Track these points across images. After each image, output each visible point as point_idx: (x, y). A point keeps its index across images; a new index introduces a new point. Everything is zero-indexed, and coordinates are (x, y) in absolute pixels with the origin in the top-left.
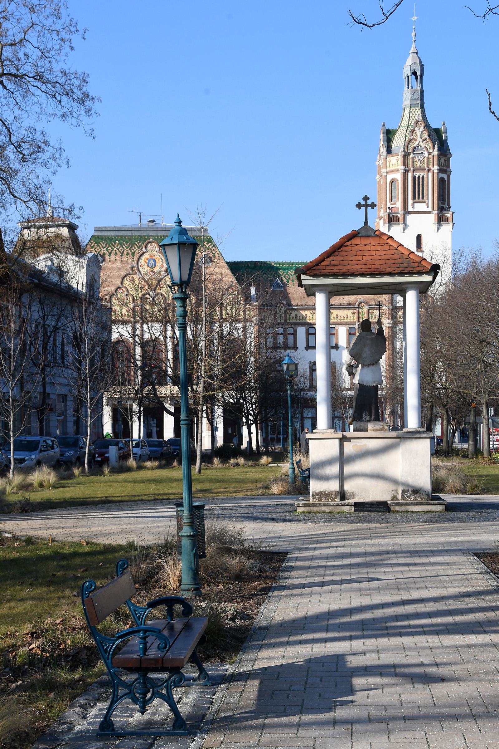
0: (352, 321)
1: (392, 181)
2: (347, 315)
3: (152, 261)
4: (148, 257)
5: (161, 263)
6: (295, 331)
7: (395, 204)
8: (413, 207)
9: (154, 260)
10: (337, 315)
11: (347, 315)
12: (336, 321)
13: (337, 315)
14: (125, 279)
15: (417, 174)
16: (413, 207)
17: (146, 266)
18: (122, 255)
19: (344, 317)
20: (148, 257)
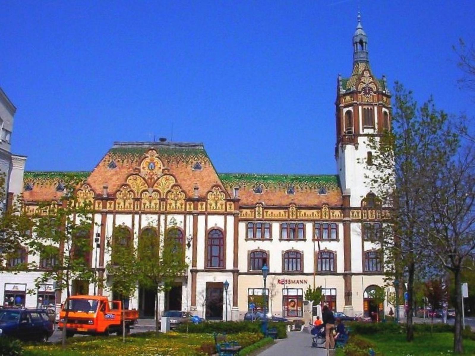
0: (317, 218)
1: (348, 112)
2: (313, 213)
3: (152, 164)
4: (149, 161)
5: (159, 166)
6: (271, 226)
7: (350, 129)
8: (363, 131)
9: (154, 164)
10: (305, 213)
11: (313, 213)
12: (304, 218)
13: (305, 213)
14: (129, 178)
15: (366, 107)
16: (363, 131)
17: (147, 168)
18: (132, 162)
19: (310, 215)
20: (149, 161)
